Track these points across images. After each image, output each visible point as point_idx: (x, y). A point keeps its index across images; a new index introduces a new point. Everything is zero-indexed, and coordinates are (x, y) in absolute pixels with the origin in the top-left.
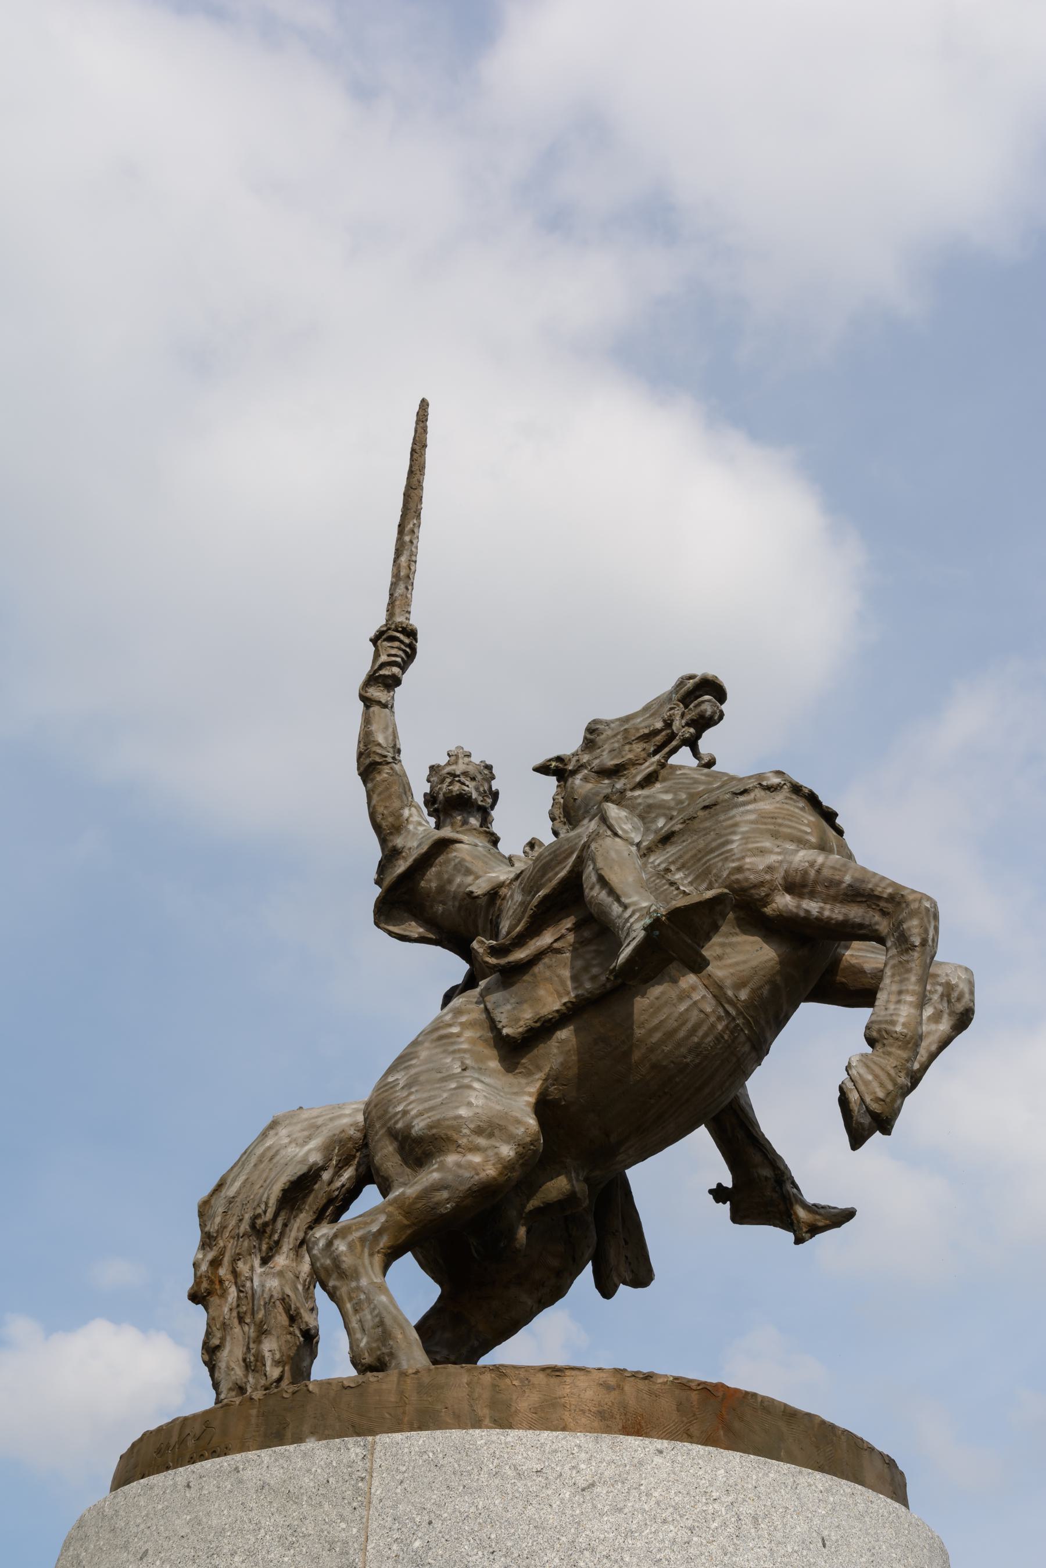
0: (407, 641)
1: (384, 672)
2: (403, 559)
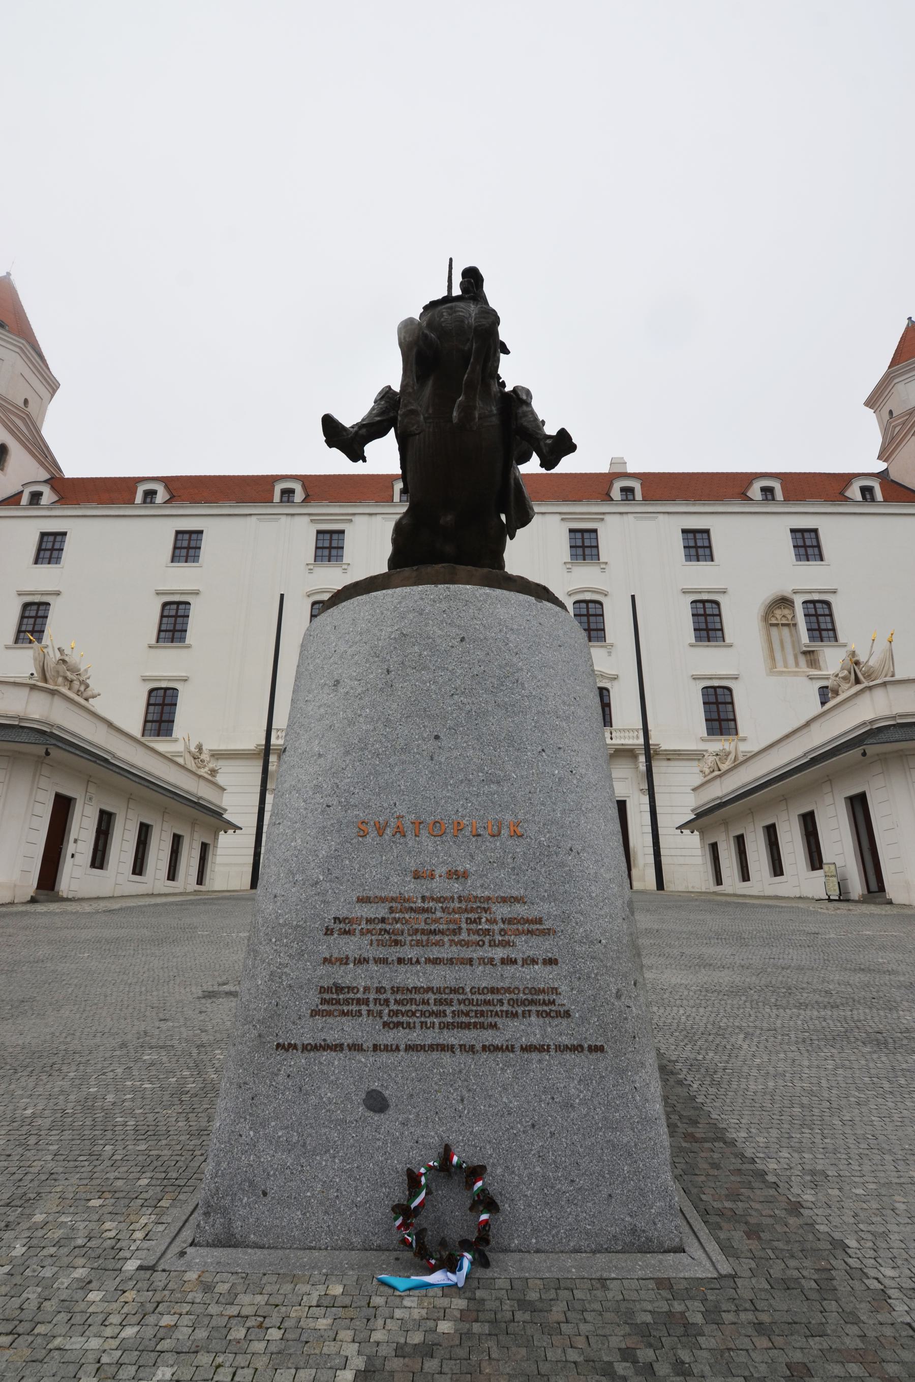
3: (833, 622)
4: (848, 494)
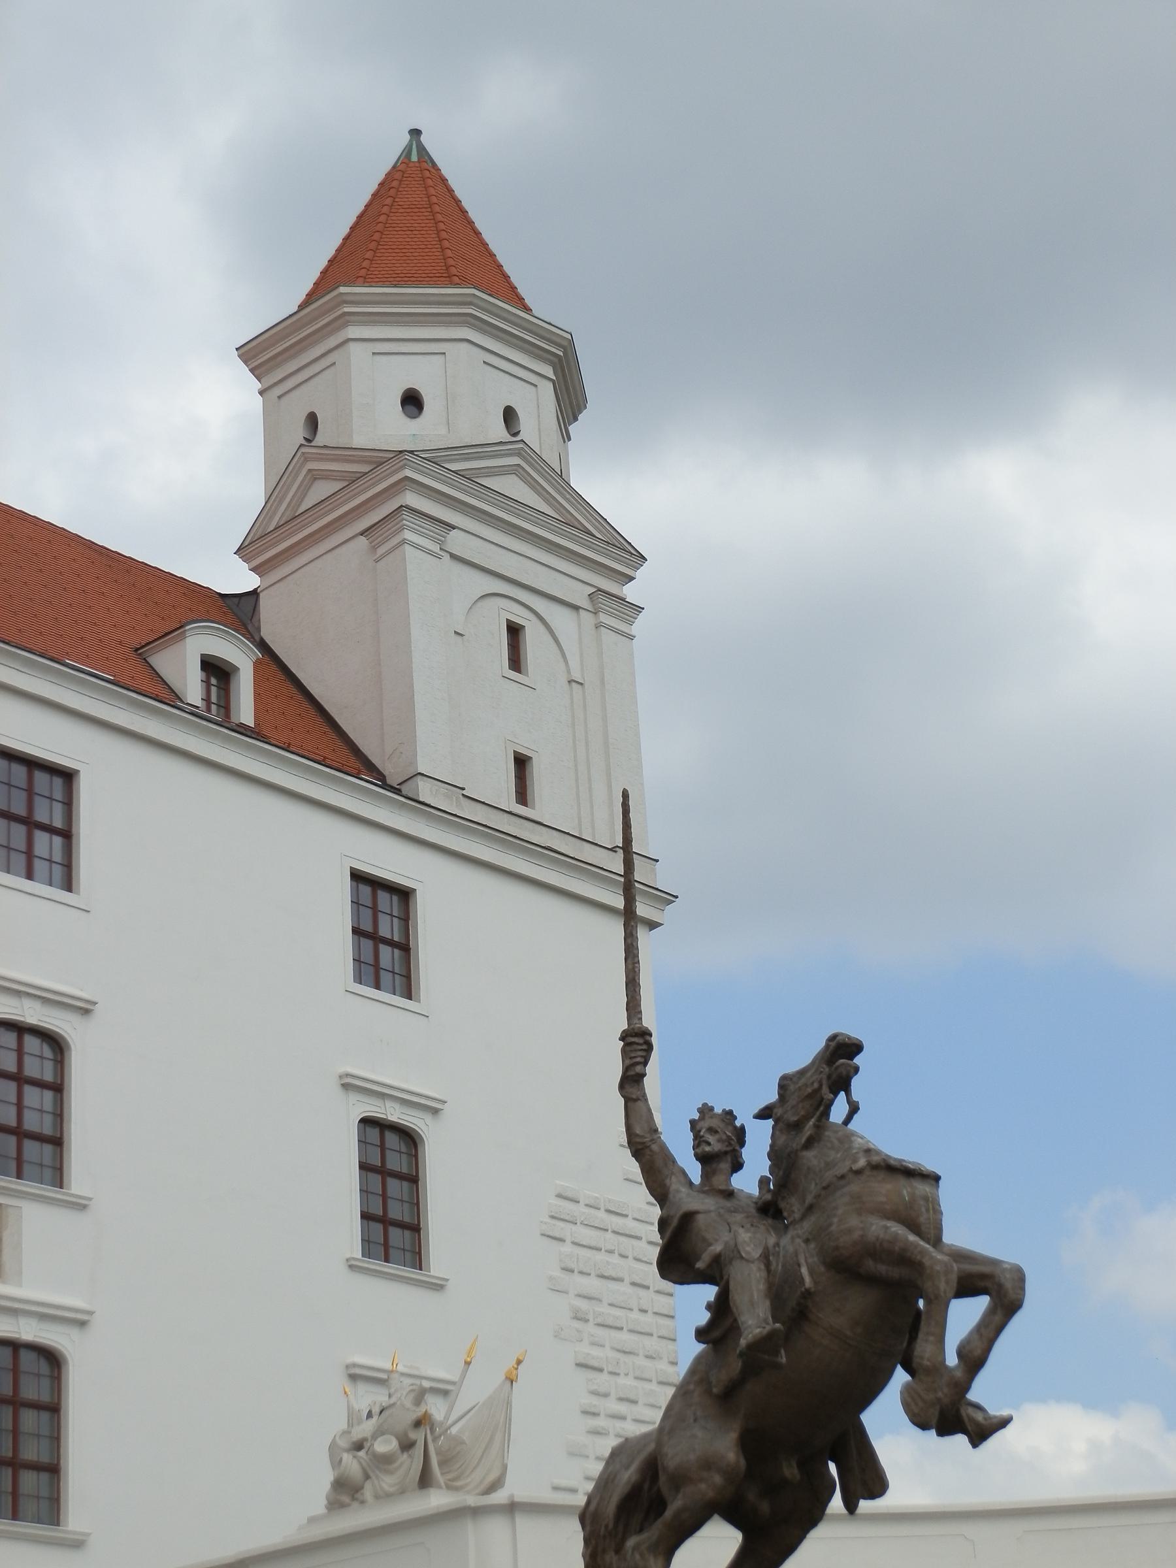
0: (641, 1041)
1: (631, 1073)
2: (629, 961)
3: (59, 1115)
4: (164, 661)
